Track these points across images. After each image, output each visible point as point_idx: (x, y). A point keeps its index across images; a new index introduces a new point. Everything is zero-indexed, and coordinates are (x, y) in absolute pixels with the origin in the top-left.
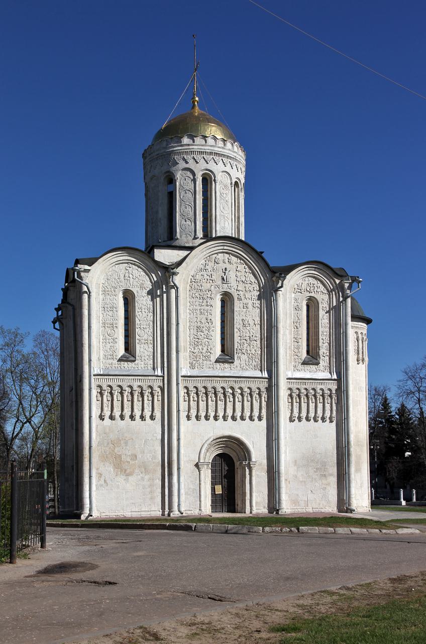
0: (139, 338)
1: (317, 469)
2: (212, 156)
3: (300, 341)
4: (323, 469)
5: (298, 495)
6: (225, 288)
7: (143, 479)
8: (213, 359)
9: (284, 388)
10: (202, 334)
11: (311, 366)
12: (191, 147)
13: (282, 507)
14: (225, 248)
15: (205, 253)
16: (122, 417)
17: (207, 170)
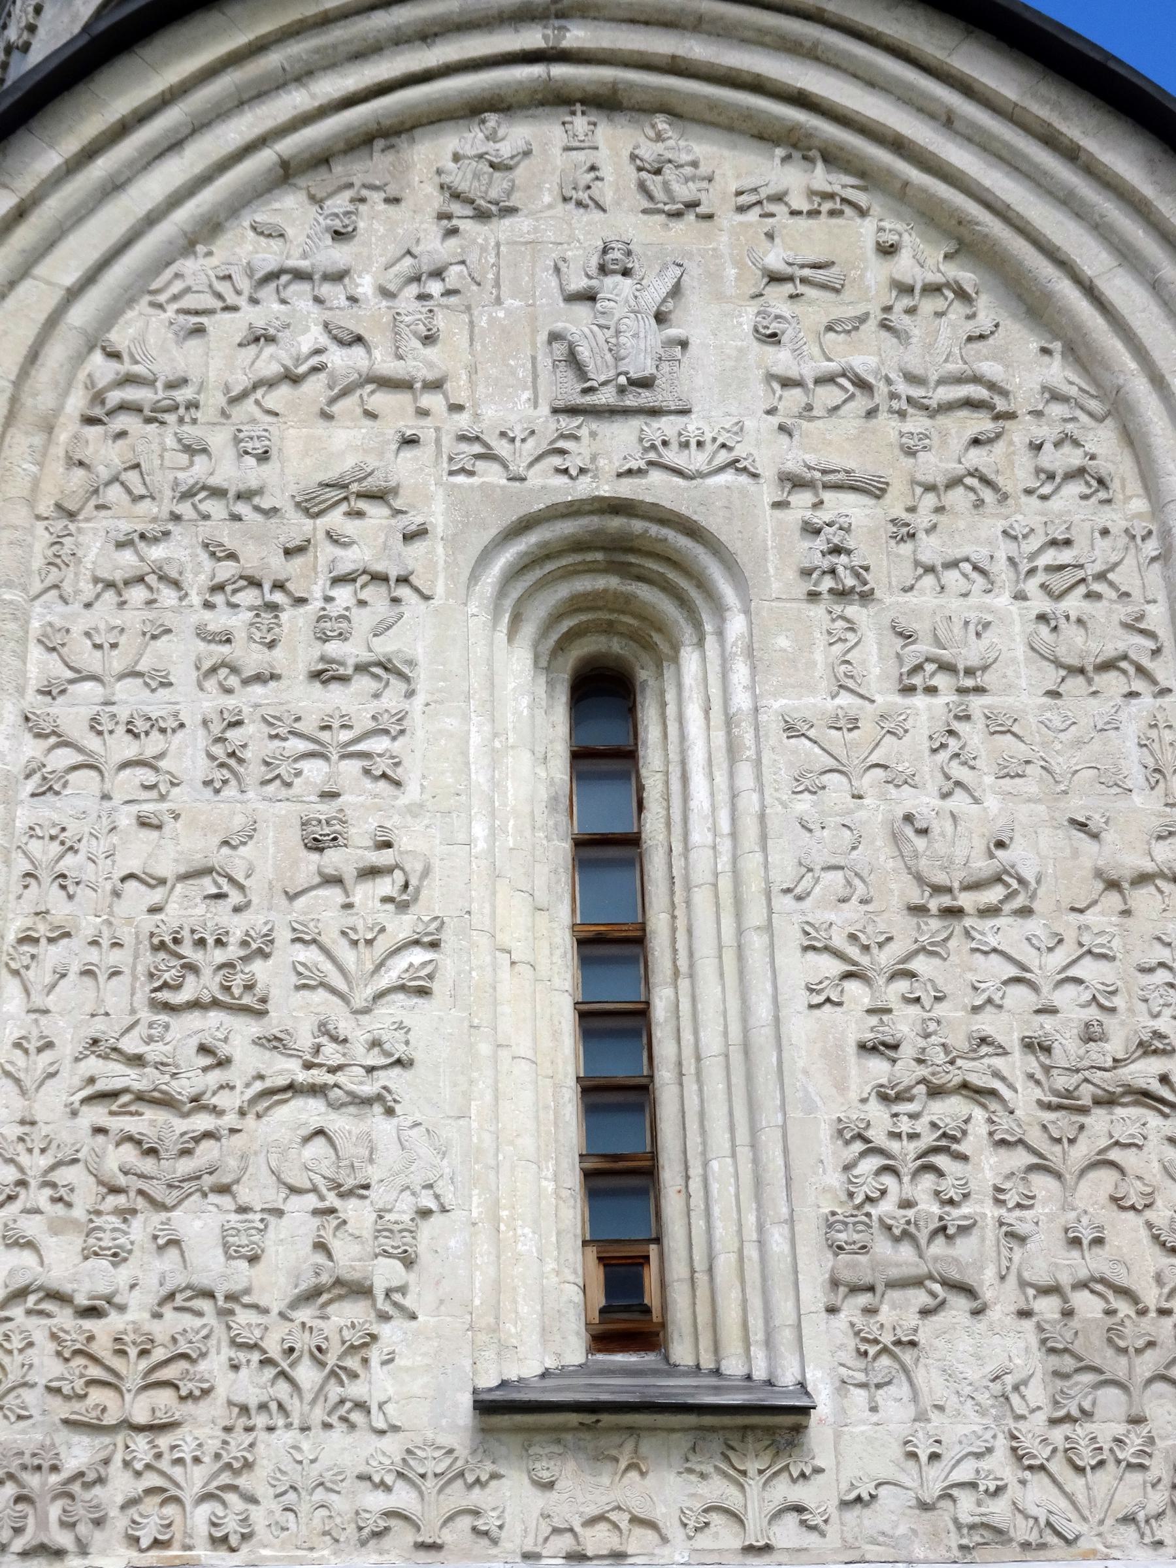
8: (423, 1386)
10: (238, 1037)
15: (297, 100)
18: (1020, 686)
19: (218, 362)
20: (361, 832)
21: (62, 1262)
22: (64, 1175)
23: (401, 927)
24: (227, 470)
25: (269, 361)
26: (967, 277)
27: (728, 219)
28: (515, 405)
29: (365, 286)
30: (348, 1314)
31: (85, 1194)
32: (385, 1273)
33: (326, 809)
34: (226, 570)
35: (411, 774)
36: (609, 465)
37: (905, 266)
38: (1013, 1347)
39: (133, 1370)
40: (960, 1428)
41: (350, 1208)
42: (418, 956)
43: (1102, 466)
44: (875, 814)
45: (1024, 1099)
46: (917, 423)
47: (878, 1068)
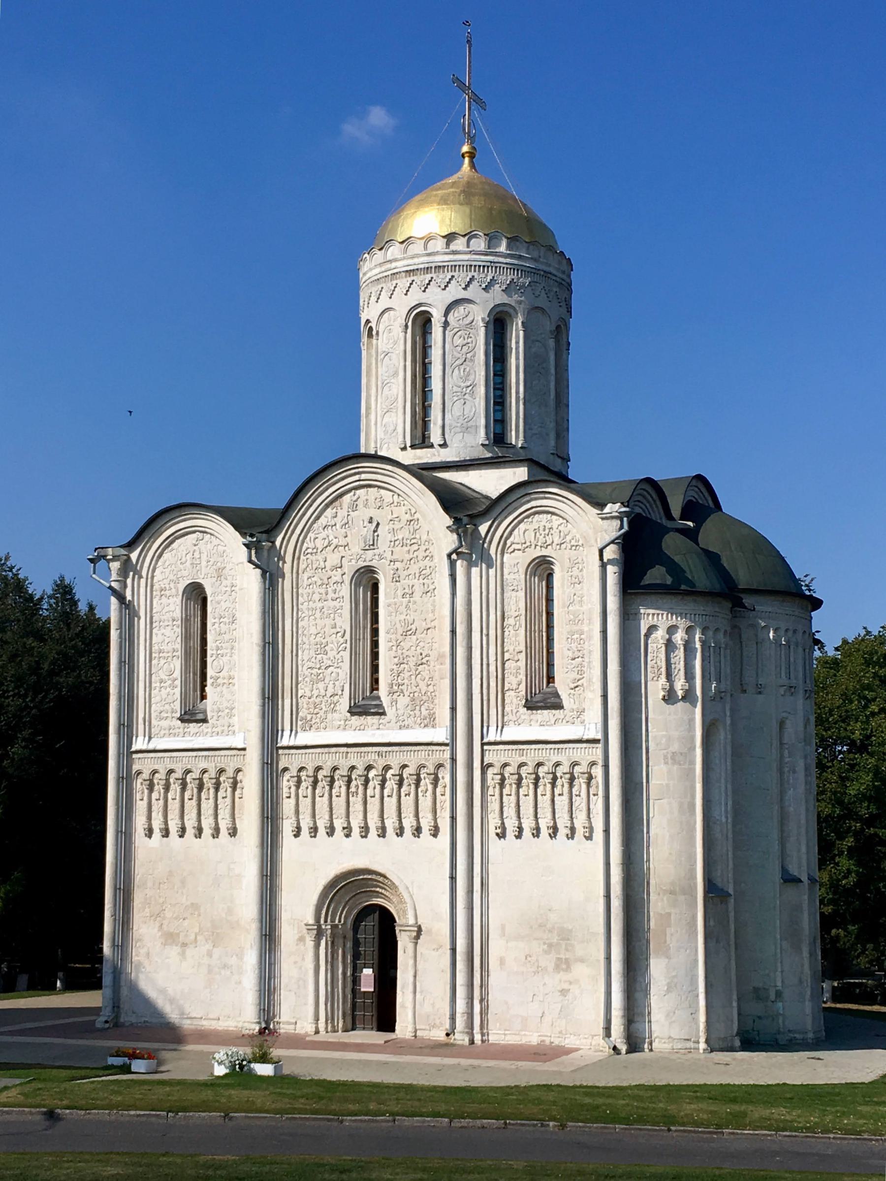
1: (550, 945)
2: (428, 277)
4: (564, 946)
5: (506, 1003)
7: (210, 954)
11: (546, 712)
12: (394, 265)
14: (363, 476)
16: (182, 832)
18: (417, 597)
23: (342, 640)
28: (356, 549)
29: (338, 526)
30: (337, 697)
33: (333, 622)
40: (400, 712)
41: (337, 683)
42: (344, 645)
45: (412, 664)
46: (409, 547)
47: (396, 660)
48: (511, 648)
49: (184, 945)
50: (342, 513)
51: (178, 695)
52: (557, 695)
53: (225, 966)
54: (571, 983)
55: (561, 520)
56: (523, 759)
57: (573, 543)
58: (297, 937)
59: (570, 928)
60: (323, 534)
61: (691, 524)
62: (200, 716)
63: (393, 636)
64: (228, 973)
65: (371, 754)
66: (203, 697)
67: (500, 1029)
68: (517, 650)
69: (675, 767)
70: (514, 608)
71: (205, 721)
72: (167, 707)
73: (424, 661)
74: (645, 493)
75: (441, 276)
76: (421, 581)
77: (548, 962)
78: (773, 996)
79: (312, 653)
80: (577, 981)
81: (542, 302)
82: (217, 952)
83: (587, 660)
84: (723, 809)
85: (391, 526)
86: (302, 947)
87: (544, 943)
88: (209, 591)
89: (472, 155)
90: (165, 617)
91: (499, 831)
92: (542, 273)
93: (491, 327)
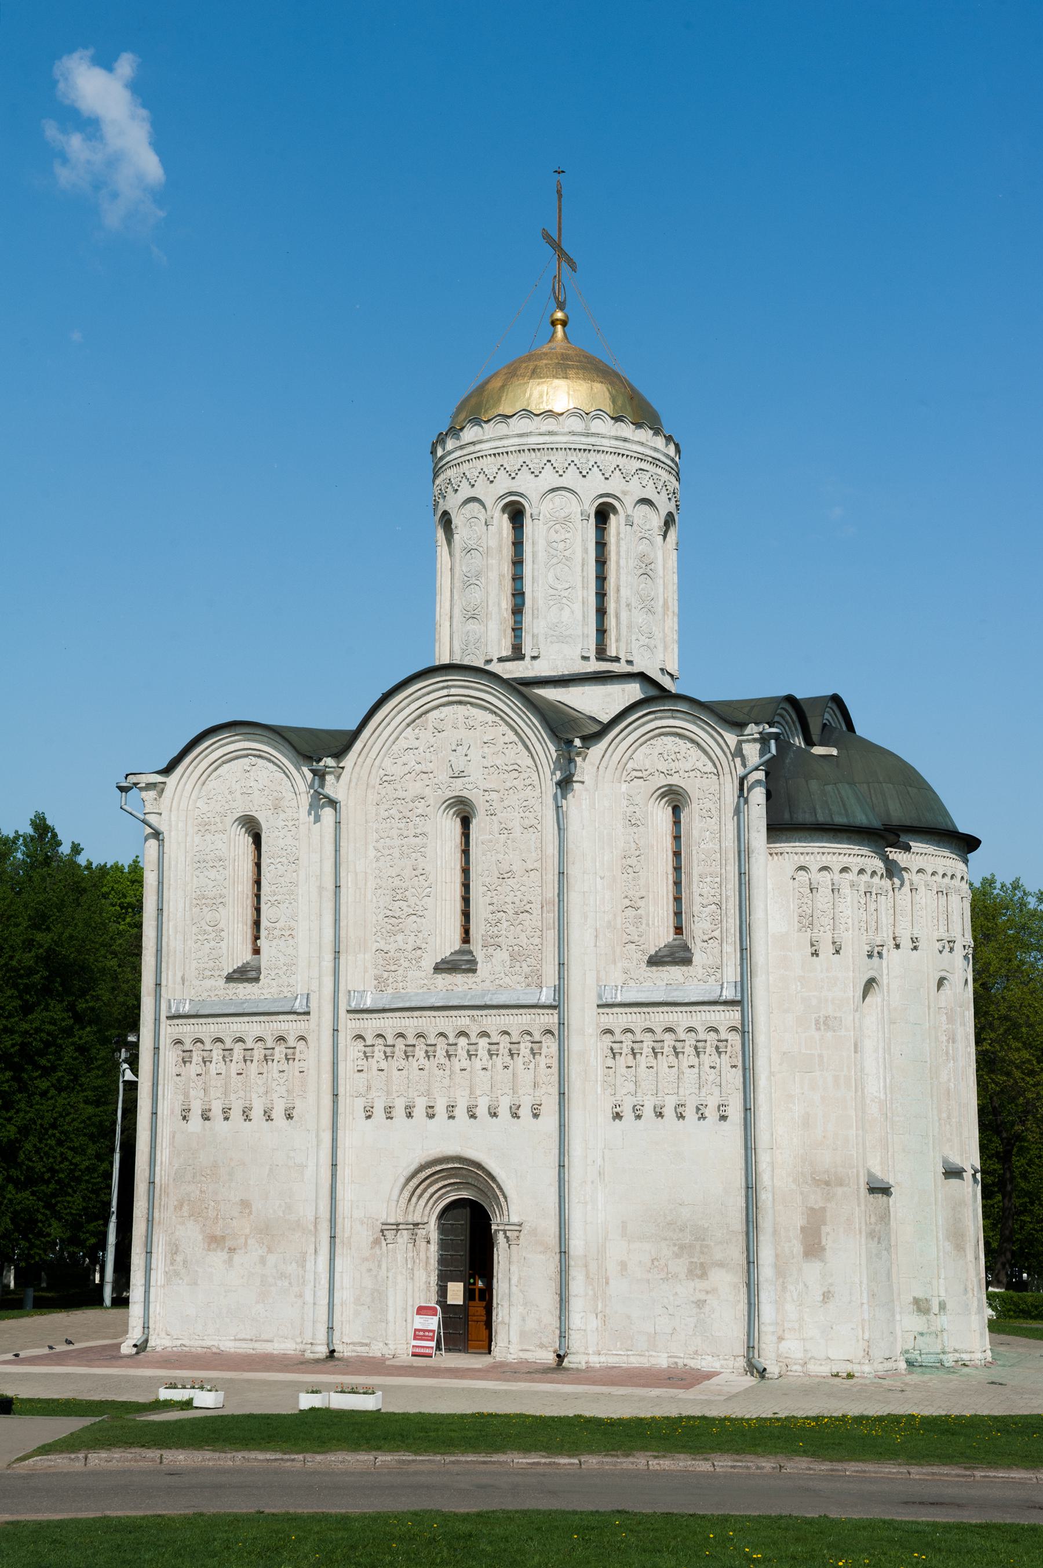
0: (269, 924)
1: (682, 1247)
3: (641, 903)
4: (698, 1247)
5: (629, 1317)
6: (458, 788)
7: (263, 1261)
9: (590, 1031)
12: (478, 447)
13: (573, 1350)
14: (453, 691)
15: (407, 711)
17: (511, 494)
19: (398, 770)
20: (420, 867)
21: (382, 945)
22: (383, 930)
23: (426, 884)
24: (401, 794)
25: (407, 769)
26: (516, 739)
27: (479, 728)
28: (443, 777)
29: (421, 750)
30: (419, 952)
31: (385, 934)
32: (423, 946)
34: (401, 816)
35: (427, 855)
36: (458, 788)
37: (507, 739)
38: (505, 956)
39: (391, 962)
43: (534, 783)
44: (494, 859)
45: (511, 912)
46: (506, 775)
48: (630, 893)
49: (232, 1250)
50: (426, 736)
51: (225, 951)
52: (686, 948)
53: (283, 1276)
54: (707, 1292)
55: (689, 745)
56: (648, 1024)
57: (704, 770)
58: (371, 1239)
59: (706, 1226)
60: (404, 759)
61: (834, 752)
62: (253, 974)
63: (488, 880)
64: (286, 1284)
65: (463, 1020)
66: (257, 951)
67: (621, 1349)
68: (638, 895)
69: (830, 1034)
70: (633, 845)
71: (257, 980)
72: (211, 963)
73: (527, 908)
74: (784, 713)
75: (536, 461)
76: (522, 814)
77: (680, 1266)
78: (935, 1309)
79: (388, 898)
80: (713, 1291)
81: (650, 493)
82: (272, 1259)
83: (724, 907)
84: (882, 1084)
85: (486, 750)
86: (378, 1252)
87: (675, 1245)
88: (264, 826)
89: (564, 323)
90: (209, 857)
91: (618, 1109)
92: (650, 459)
93: (592, 520)
